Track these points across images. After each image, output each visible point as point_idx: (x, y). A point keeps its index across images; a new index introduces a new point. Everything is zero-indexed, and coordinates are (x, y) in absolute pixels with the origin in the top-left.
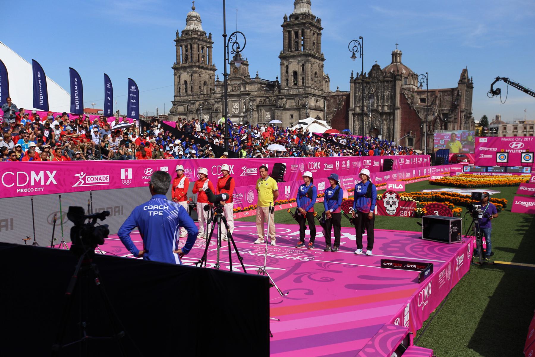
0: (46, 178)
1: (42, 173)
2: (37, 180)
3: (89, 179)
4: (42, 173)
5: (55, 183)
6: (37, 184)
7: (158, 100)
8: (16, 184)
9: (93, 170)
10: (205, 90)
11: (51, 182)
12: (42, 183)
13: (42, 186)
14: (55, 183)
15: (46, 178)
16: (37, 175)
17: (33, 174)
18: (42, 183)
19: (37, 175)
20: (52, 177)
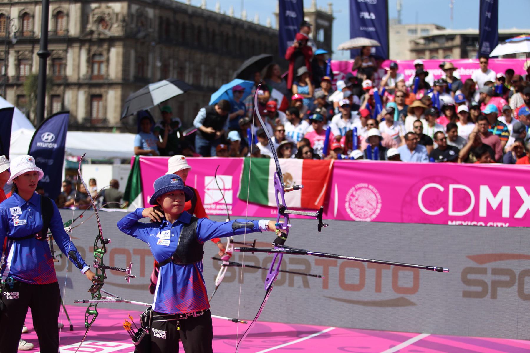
1: (505, 192)
2: (494, 206)
4: (505, 192)
6: (494, 214)
12: (506, 213)
13: (505, 220)
16: (495, 193)
17: (485, 191)
18: (506, 213)
19: (495, 193)
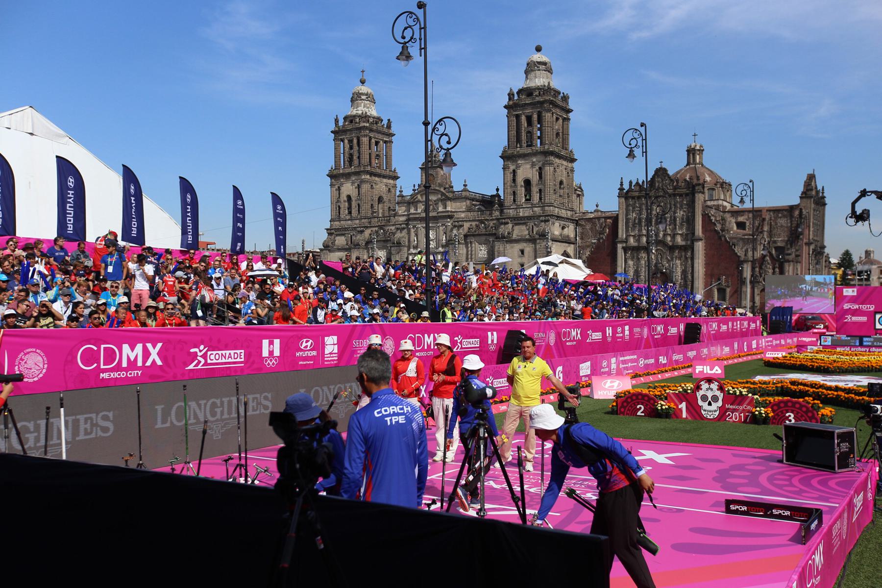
0: (146, 354)
2: (132, 359)
3: (212, 357)
5: (159, 363)
6: (132, 364)
7: (309, 232)
8: (99, 365)
9: (219, 341)
10: (381, 210)
11: (154, 361)
12: (140, 364)
13: (139, 368)
14: (159, 363)
15: (146, 354)
16: (132, 349)
18: (140, 364)
19: (132, 349)
20: (154, 355)
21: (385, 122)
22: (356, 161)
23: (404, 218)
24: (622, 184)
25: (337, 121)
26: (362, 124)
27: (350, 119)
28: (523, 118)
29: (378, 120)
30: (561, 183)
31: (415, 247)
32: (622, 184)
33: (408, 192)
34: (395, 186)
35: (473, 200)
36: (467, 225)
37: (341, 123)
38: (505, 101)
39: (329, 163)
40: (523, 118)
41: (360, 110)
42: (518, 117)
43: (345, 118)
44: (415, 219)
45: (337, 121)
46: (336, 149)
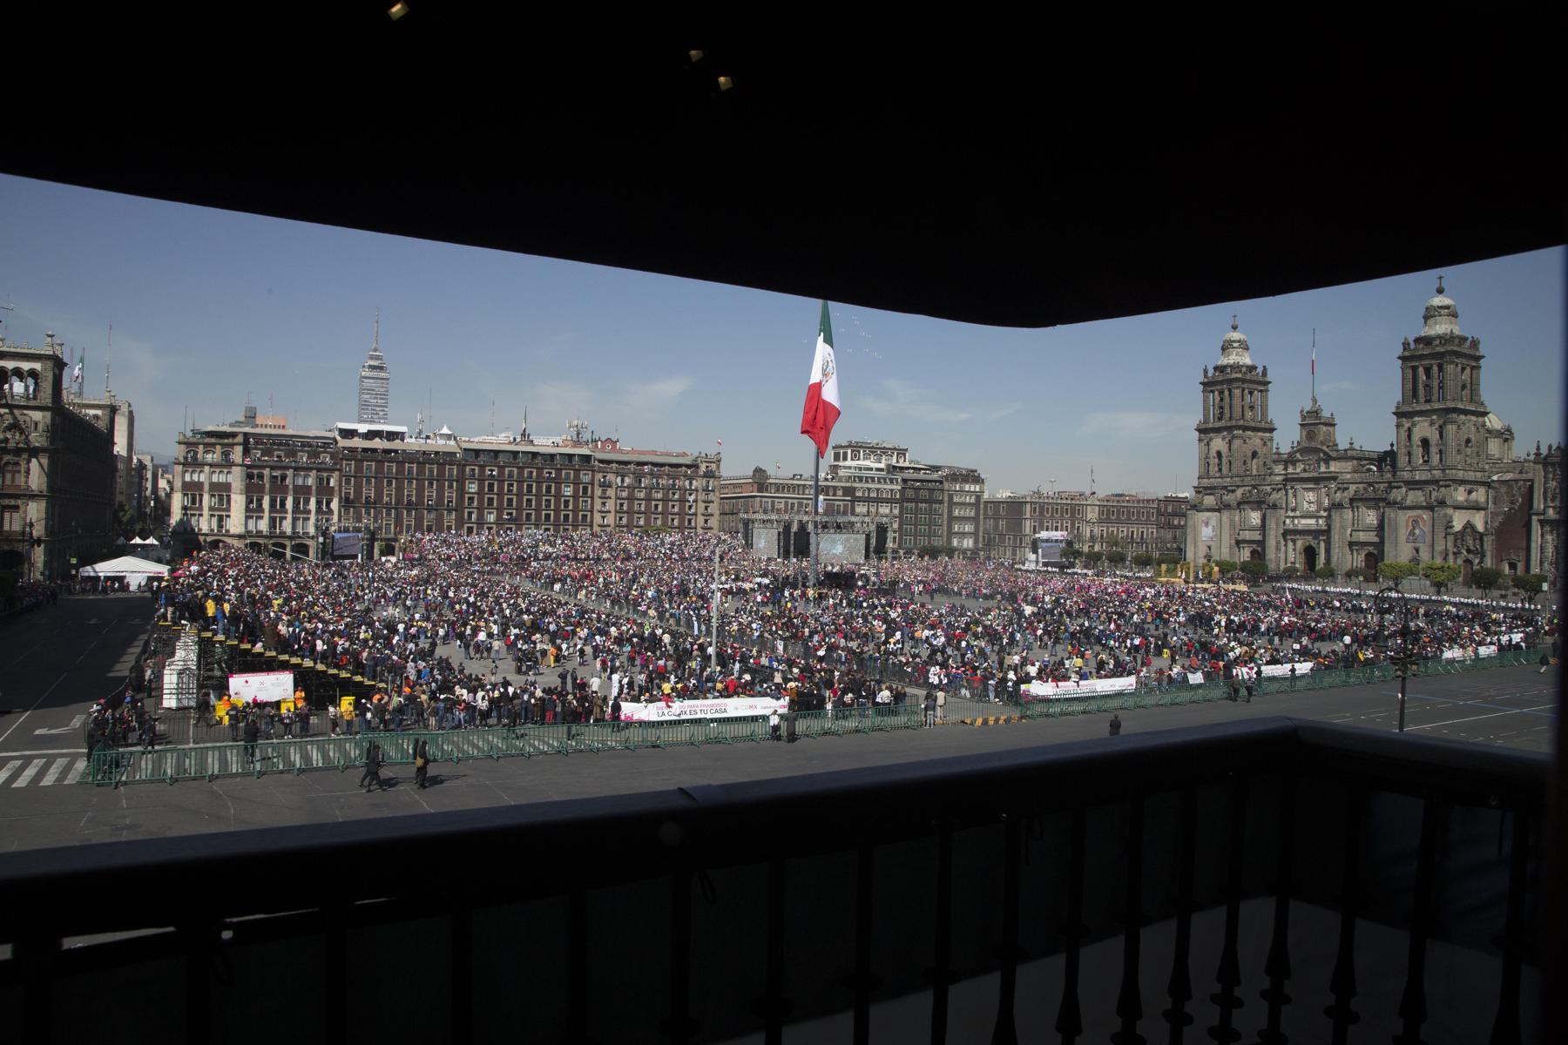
21: (1260, 370)
22: (1227, 415)
23: (1280, 478)
24: (1538, 448)
25: (1206, 371)
26: (1235, 375)
27: (1220, 369)
28: (1421, 370)
29: (1252, 368)
30: (1468, 441)
31: (1294, 510)
32: (1538, 448)
33: (1285, 449)
34: (1271, 439)
35: (1359, 459)
36: (1353, 488)
37: (1210, 374)
38: (1399, 351)
39: (1197, 417)
40: (1421, 370)
41: (1232, 359)
42: (1414, 369)
43: (1216, 368)
44: (1293, 480)
45: (1206, 371)
46: (1205, 401)
